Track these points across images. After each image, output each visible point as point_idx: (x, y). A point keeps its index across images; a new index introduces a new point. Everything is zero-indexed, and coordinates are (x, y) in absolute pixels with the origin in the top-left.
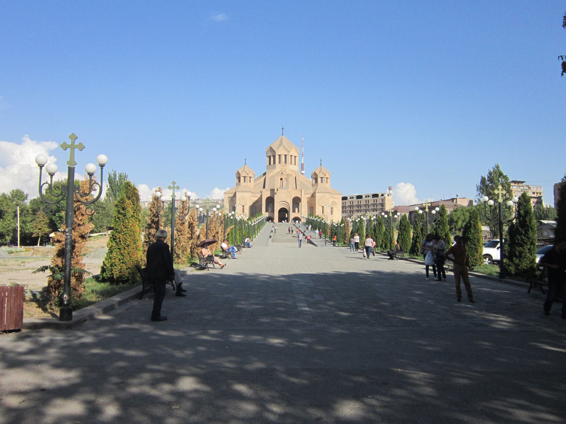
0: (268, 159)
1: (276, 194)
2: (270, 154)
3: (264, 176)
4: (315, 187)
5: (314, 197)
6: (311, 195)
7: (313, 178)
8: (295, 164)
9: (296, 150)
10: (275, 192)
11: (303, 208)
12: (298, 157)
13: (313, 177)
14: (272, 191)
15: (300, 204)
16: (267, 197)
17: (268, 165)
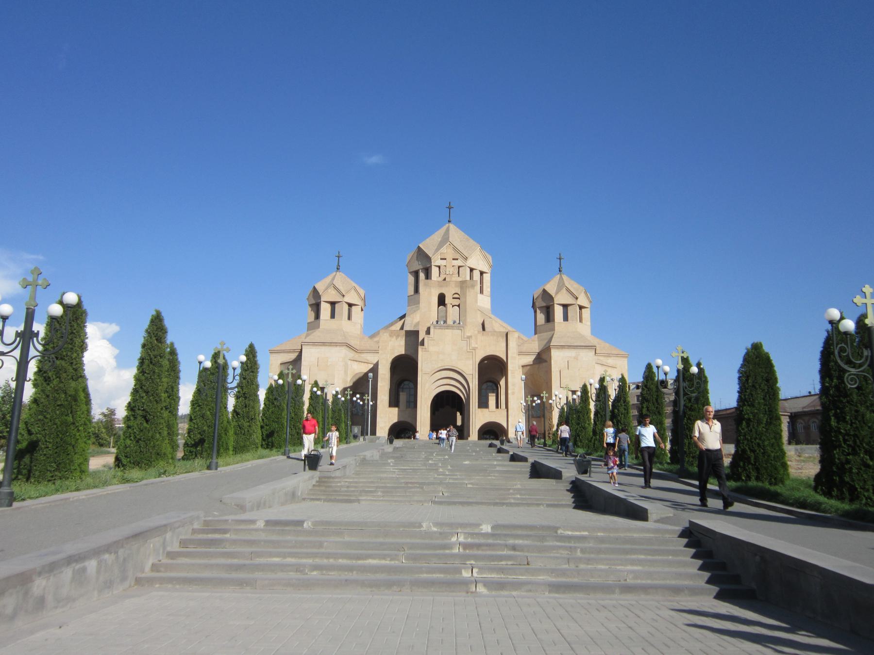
0: (411, 279)
1: (423, 343)
2: (417, 266)
3: (400, 320)
4: (545, 334)
5: (546, 361)
6: (533, 357)
7: (540, 308)
8: (481, 292)
9: (485, 257)
10: (420, 339)
11: (513, 393)
12: (489, 274)
13: (537, 304)
14: (413, 338)
15: (502, 382)
16: (393, 356)
17: (412, 293)
